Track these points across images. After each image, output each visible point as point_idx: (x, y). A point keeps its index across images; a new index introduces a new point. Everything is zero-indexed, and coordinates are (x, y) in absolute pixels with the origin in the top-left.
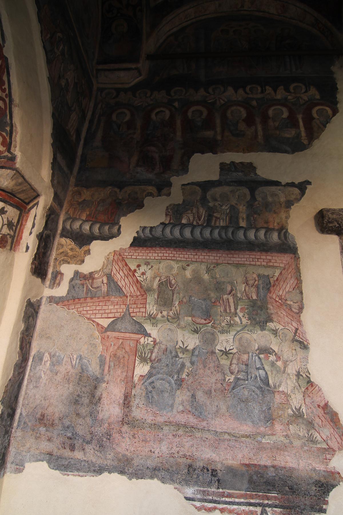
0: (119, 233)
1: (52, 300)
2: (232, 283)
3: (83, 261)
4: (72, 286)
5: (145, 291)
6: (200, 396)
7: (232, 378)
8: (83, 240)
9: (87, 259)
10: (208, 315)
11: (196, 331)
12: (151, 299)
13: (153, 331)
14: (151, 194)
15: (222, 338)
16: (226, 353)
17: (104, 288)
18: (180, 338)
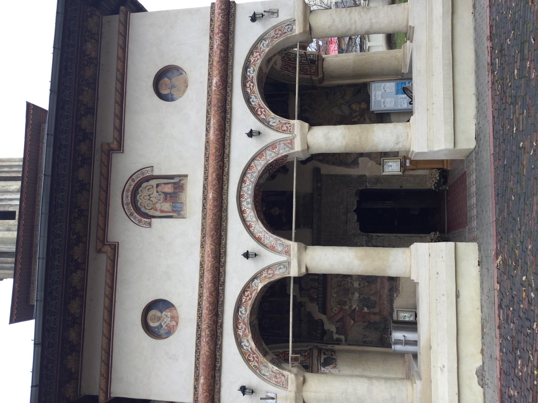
0: (321, 320)
1: (346, 341)
2: (338, 282)
3: (332, 332)
4: (342, 334)
5: (341, 309)
6: (372, 293)
7: (366, 283)
8: (324, 332)
9: (331, 330)
10: (348, 290)
11: (354, 293)
12: (344, 308)
13: (354, 306)
14: (305, 309)
15: (355, 286)
16: (359, 285)
17: (341, 323)
18: (356, 298)
